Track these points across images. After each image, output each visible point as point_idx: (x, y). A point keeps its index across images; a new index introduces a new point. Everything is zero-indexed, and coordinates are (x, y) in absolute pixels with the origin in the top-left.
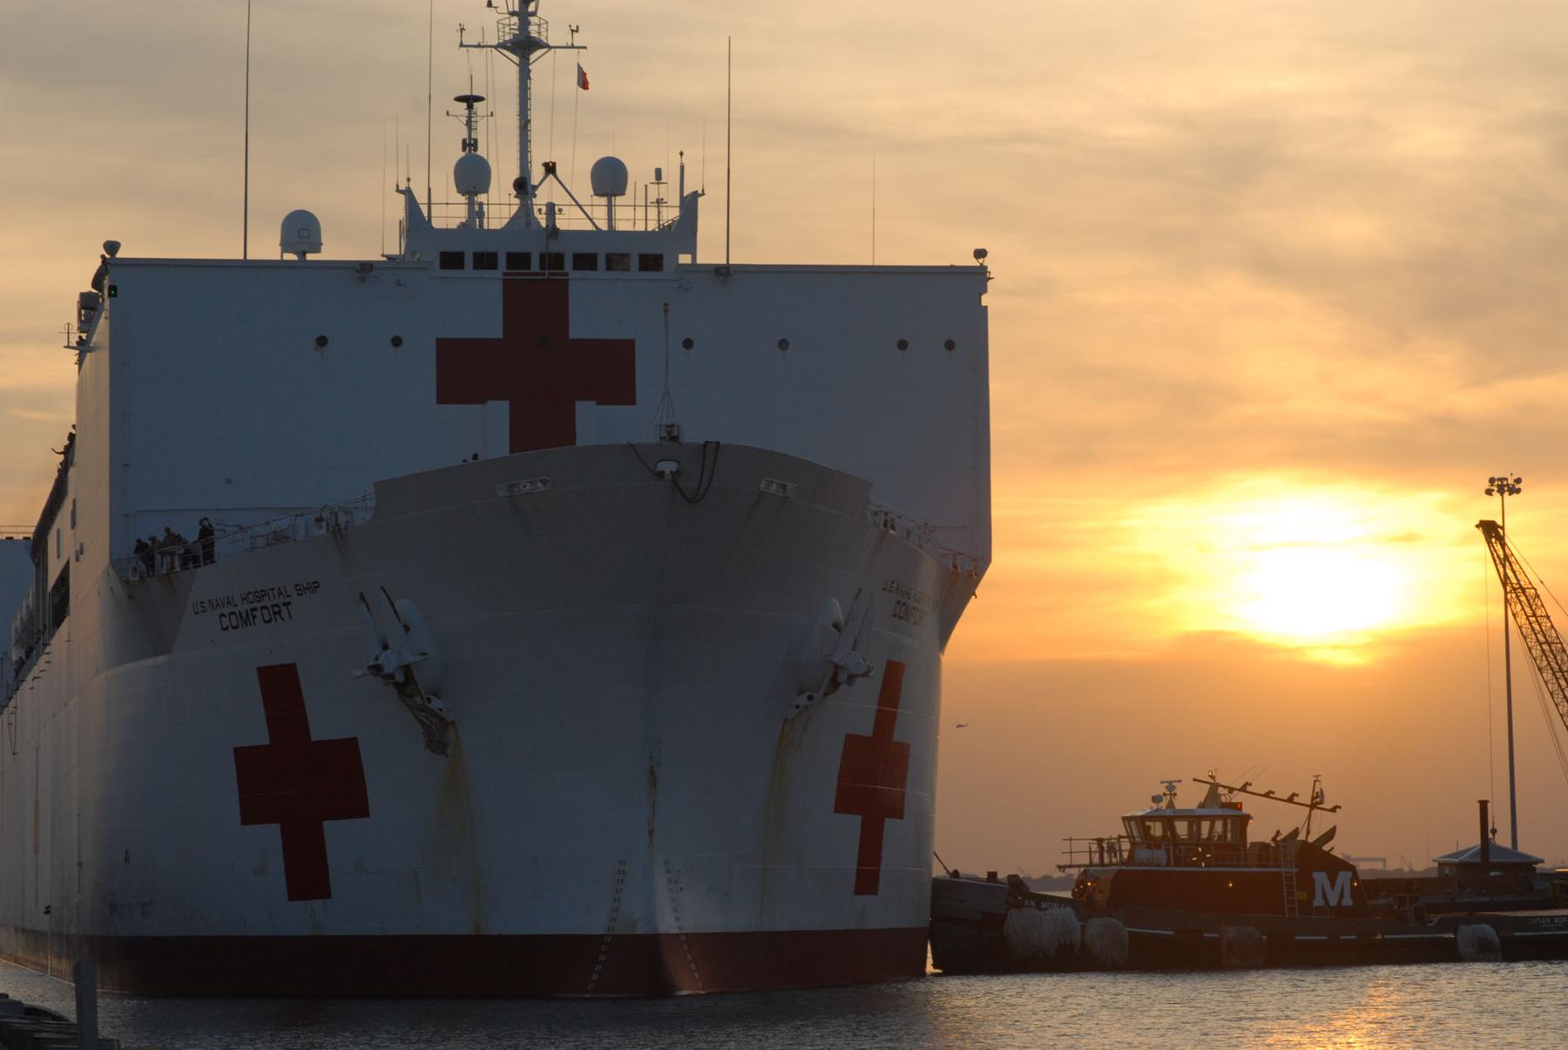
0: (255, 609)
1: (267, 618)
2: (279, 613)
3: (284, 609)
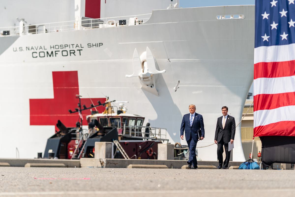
0: (59, 51)
3: (77, 53)
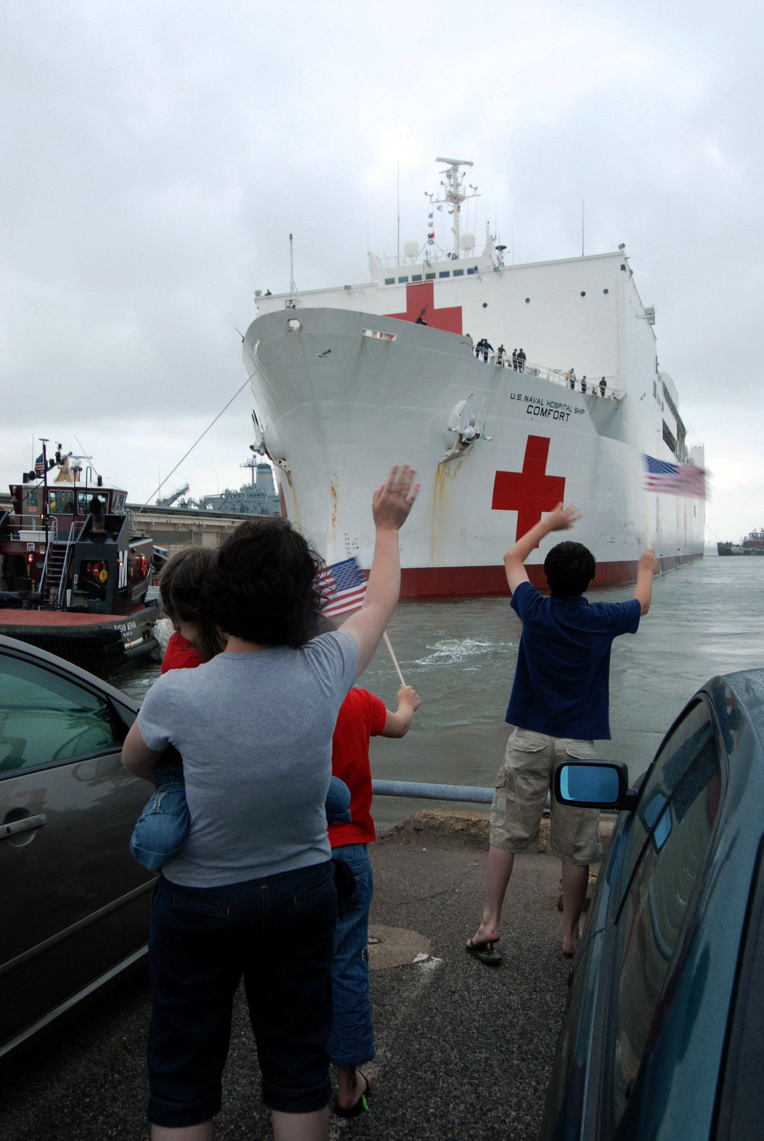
0: (552, 411)
2: (563, 417)
3: (566, 416)
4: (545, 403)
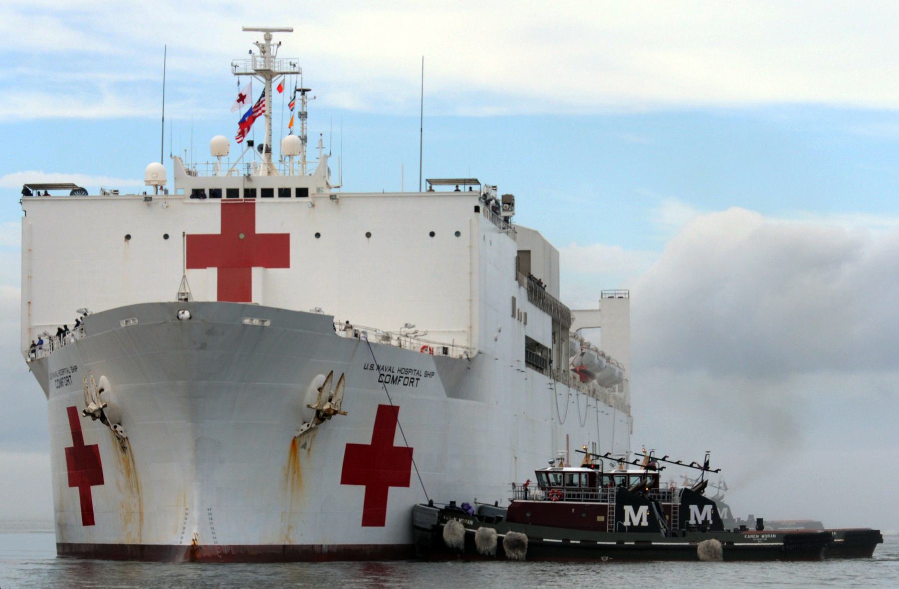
0: (402, 377)
1: (406, 383)
2: (412, 382)
3: (416, 381)
4: (396, 370)
